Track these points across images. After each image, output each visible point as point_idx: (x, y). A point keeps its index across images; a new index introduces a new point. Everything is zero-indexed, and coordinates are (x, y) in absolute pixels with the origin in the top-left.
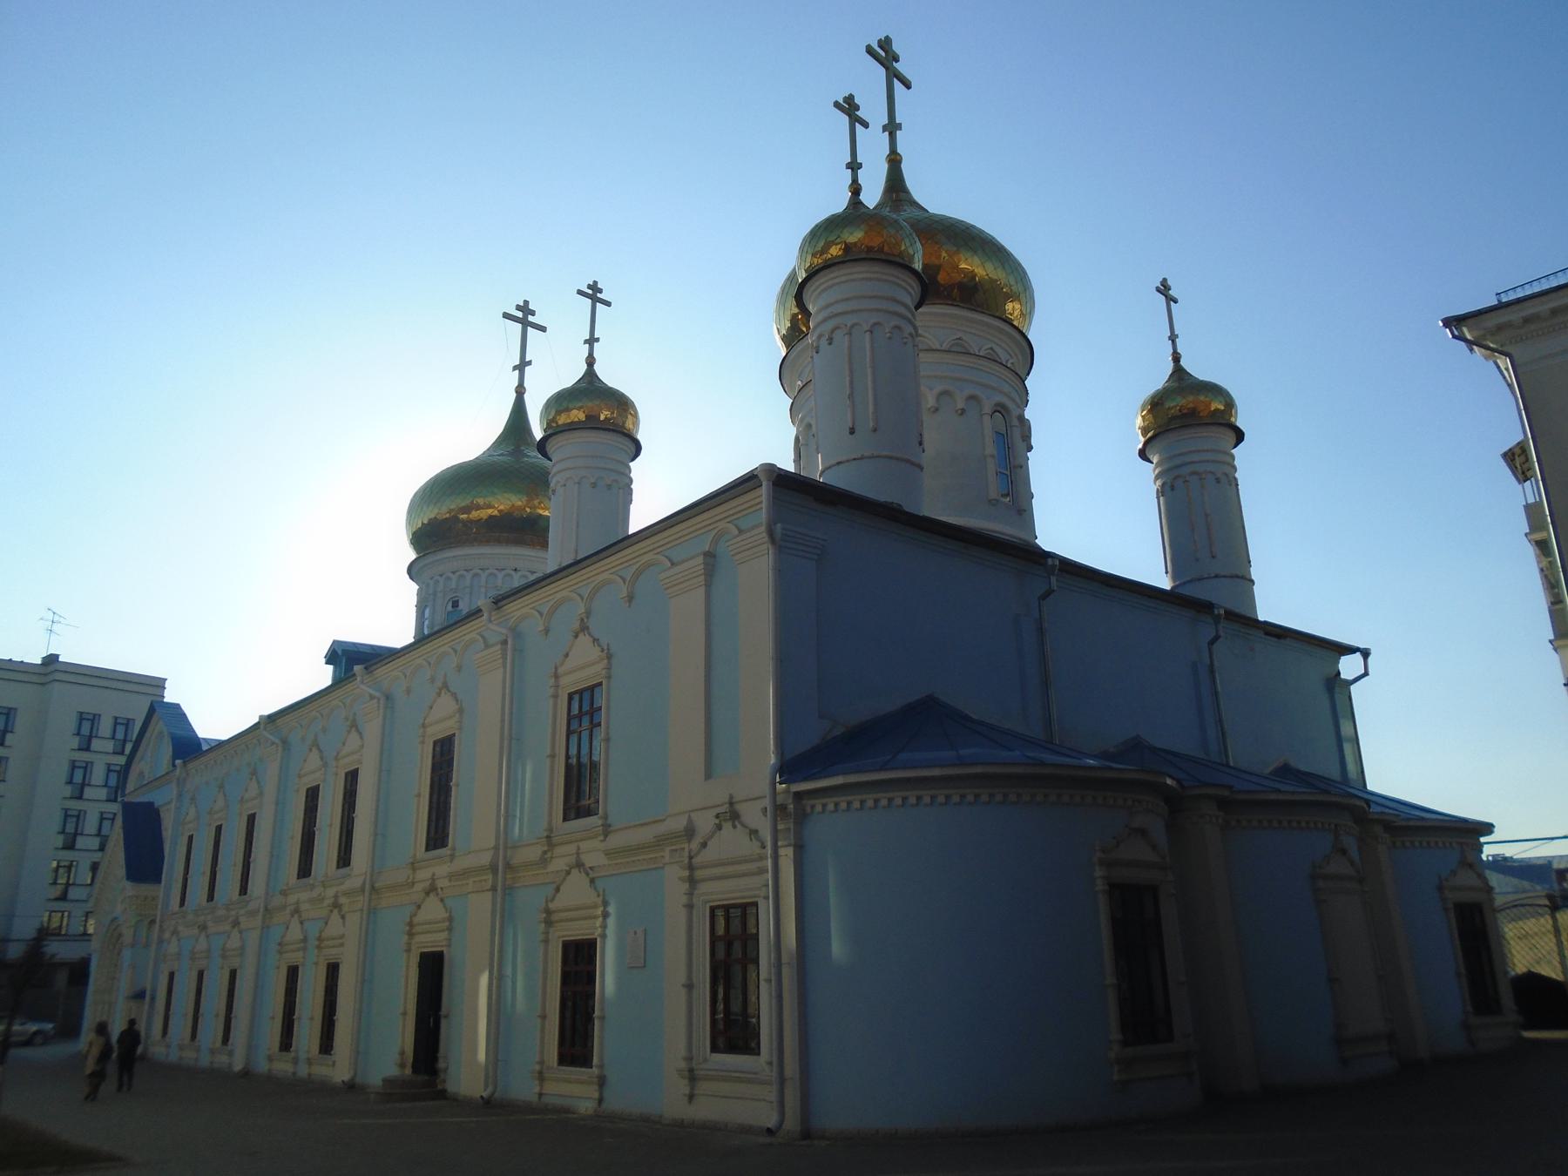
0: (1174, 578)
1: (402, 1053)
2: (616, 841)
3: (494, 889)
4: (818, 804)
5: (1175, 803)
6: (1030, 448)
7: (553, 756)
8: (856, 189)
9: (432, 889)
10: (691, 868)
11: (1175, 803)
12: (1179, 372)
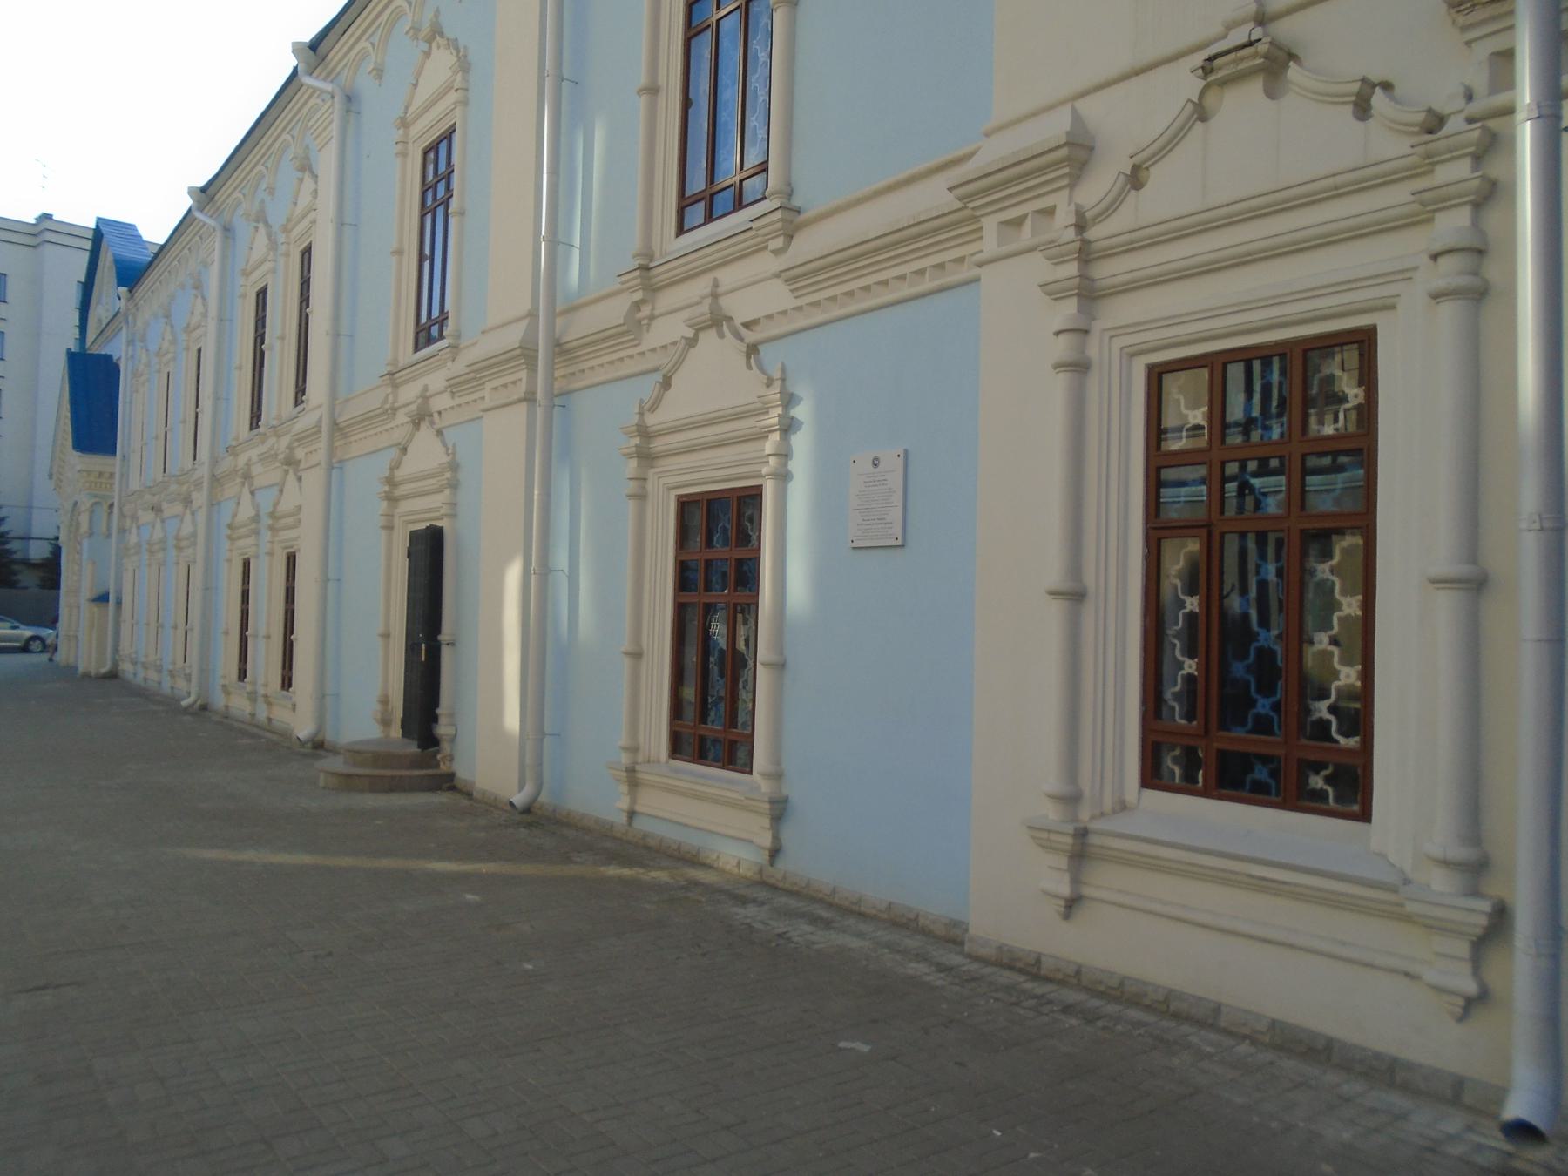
1: (385, 701)
2: (810, 245)
3: (529, 398)
7: (652, 90)
9: (420, 418)
10: (1086, 255)
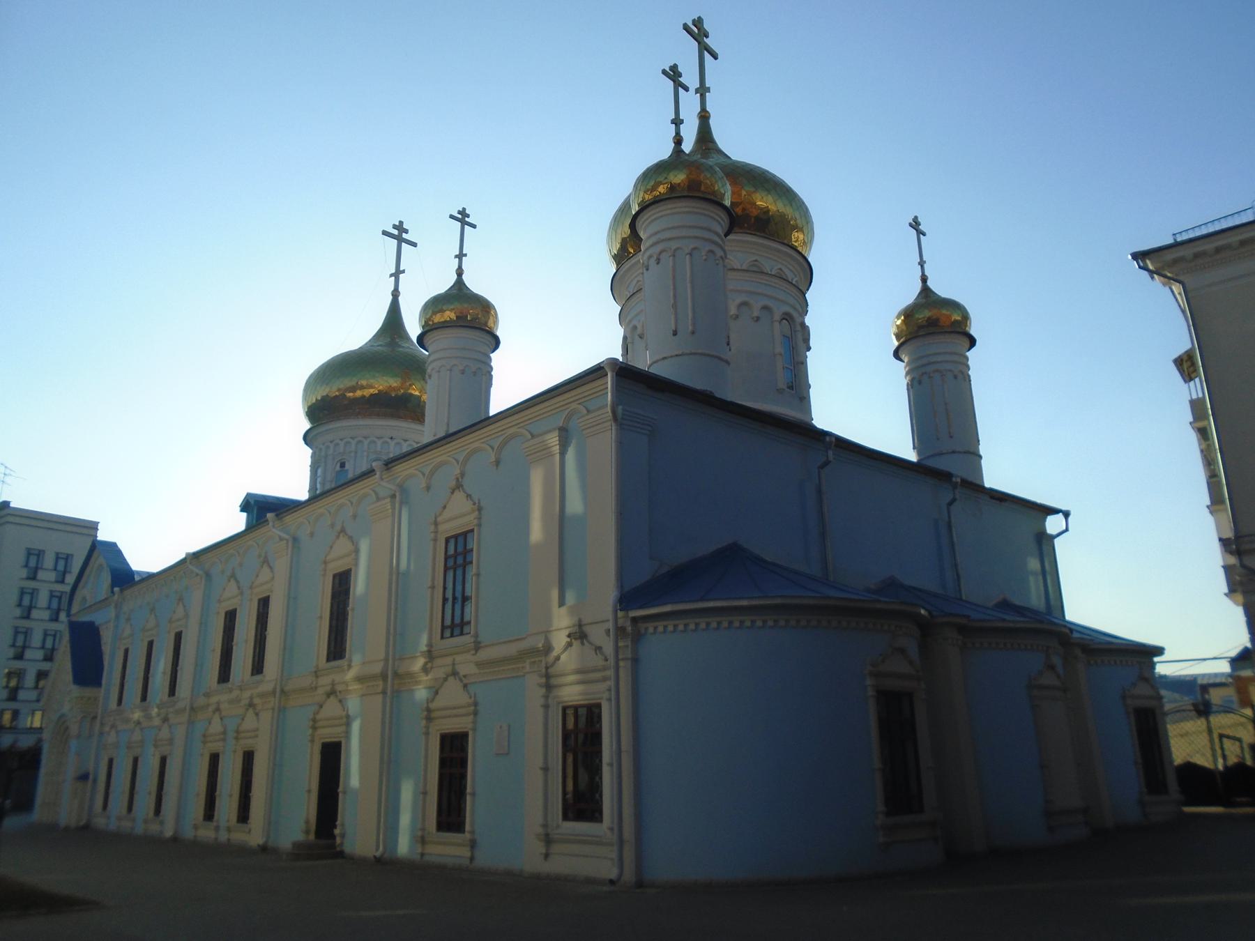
0: (919, 454)
1: (307, 822)
2: (484, 655)
3: (384, 692)
4: (651, 627)
5: (926, 629)
6: (809, 349)
7: (433, 587)
8: (678, 141)
9: (332, 693)
10: (548, 676)
11: (926, 629)
12: (926, 291)
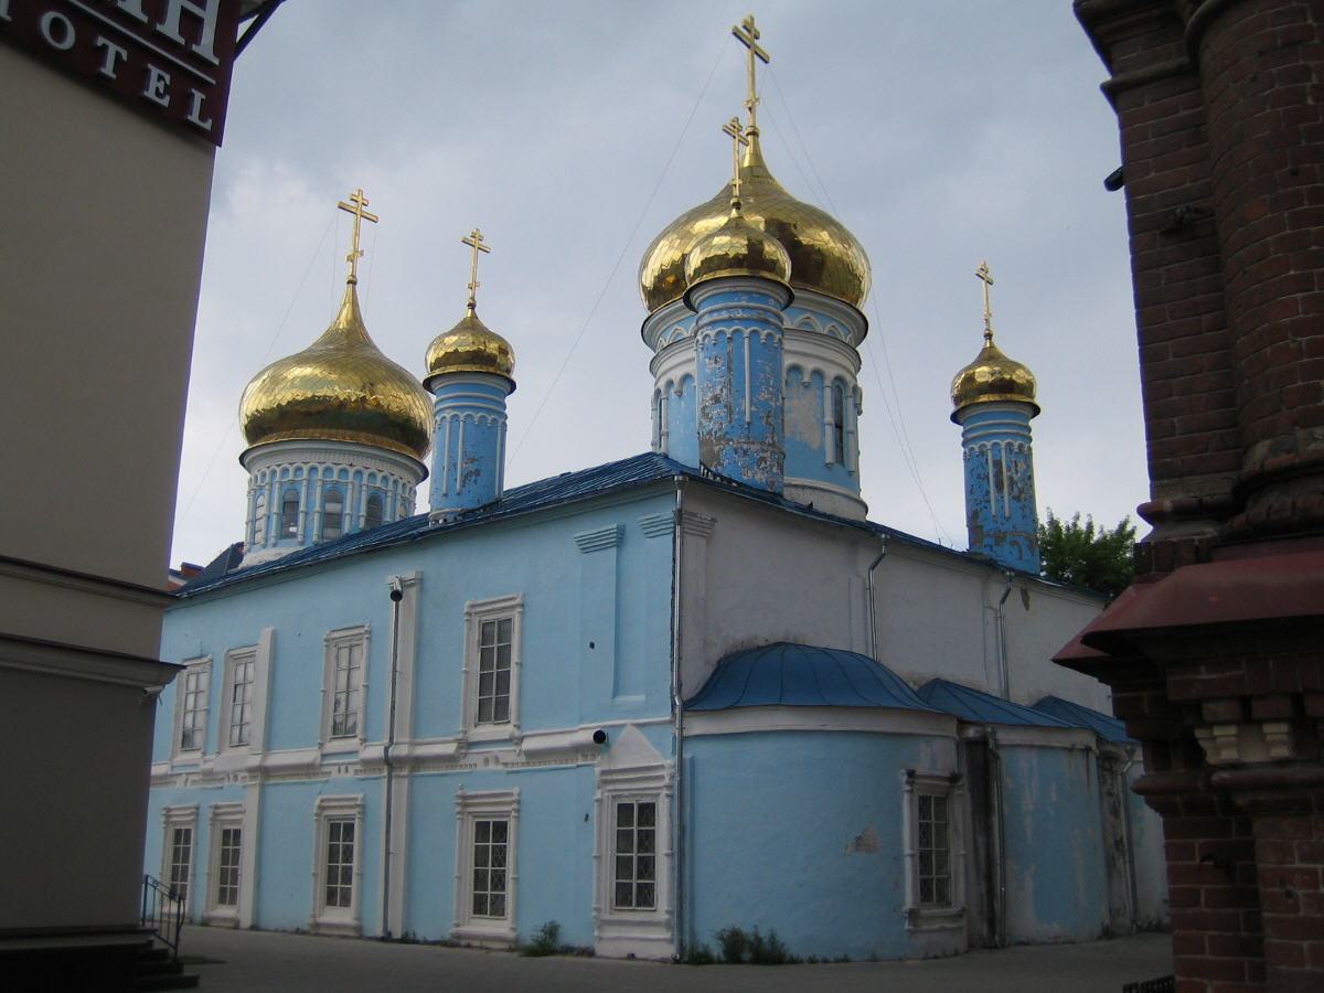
2: (528, 745)
